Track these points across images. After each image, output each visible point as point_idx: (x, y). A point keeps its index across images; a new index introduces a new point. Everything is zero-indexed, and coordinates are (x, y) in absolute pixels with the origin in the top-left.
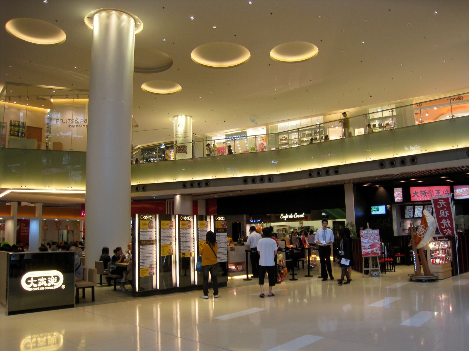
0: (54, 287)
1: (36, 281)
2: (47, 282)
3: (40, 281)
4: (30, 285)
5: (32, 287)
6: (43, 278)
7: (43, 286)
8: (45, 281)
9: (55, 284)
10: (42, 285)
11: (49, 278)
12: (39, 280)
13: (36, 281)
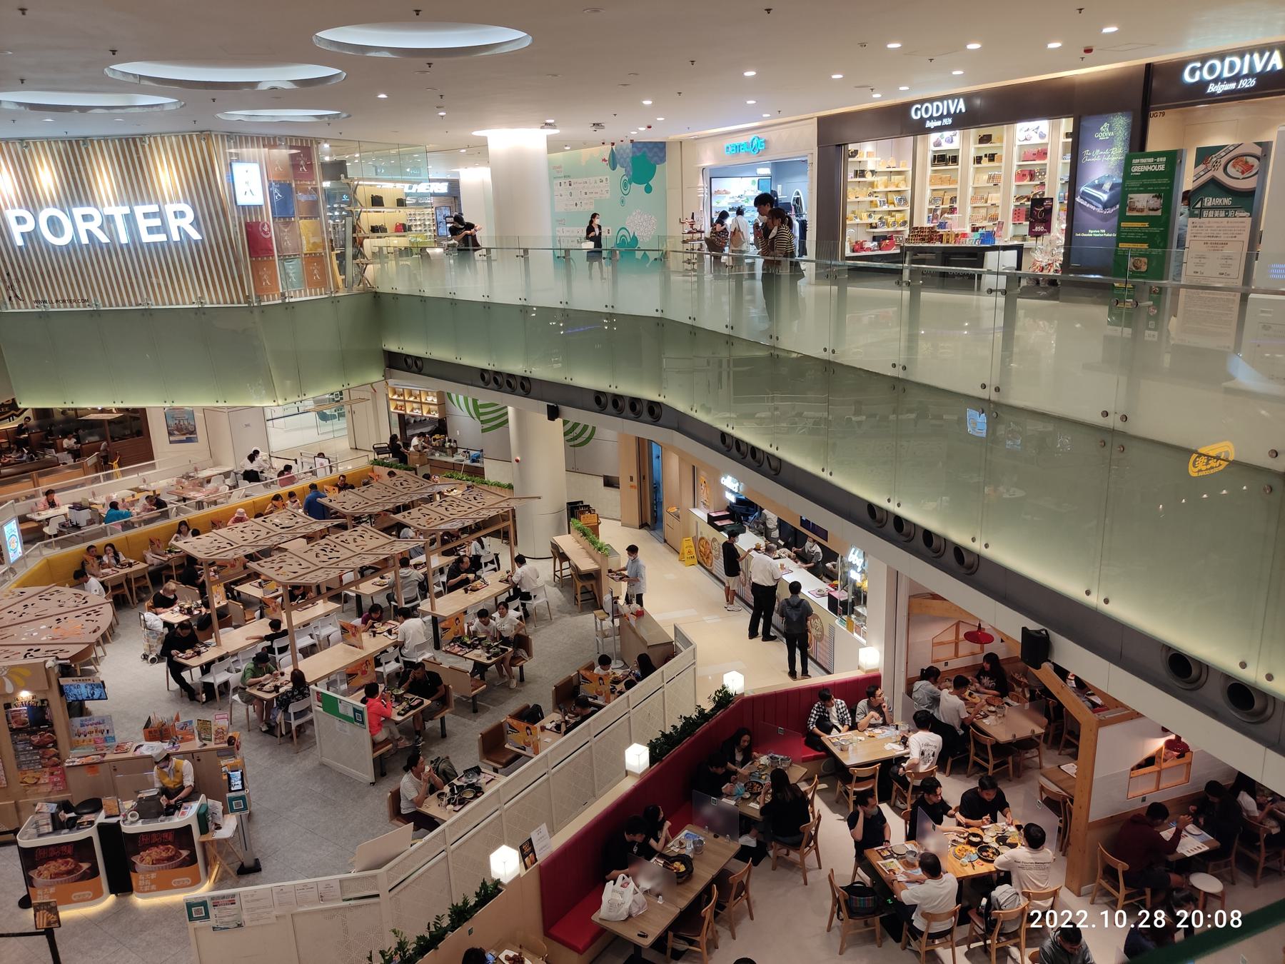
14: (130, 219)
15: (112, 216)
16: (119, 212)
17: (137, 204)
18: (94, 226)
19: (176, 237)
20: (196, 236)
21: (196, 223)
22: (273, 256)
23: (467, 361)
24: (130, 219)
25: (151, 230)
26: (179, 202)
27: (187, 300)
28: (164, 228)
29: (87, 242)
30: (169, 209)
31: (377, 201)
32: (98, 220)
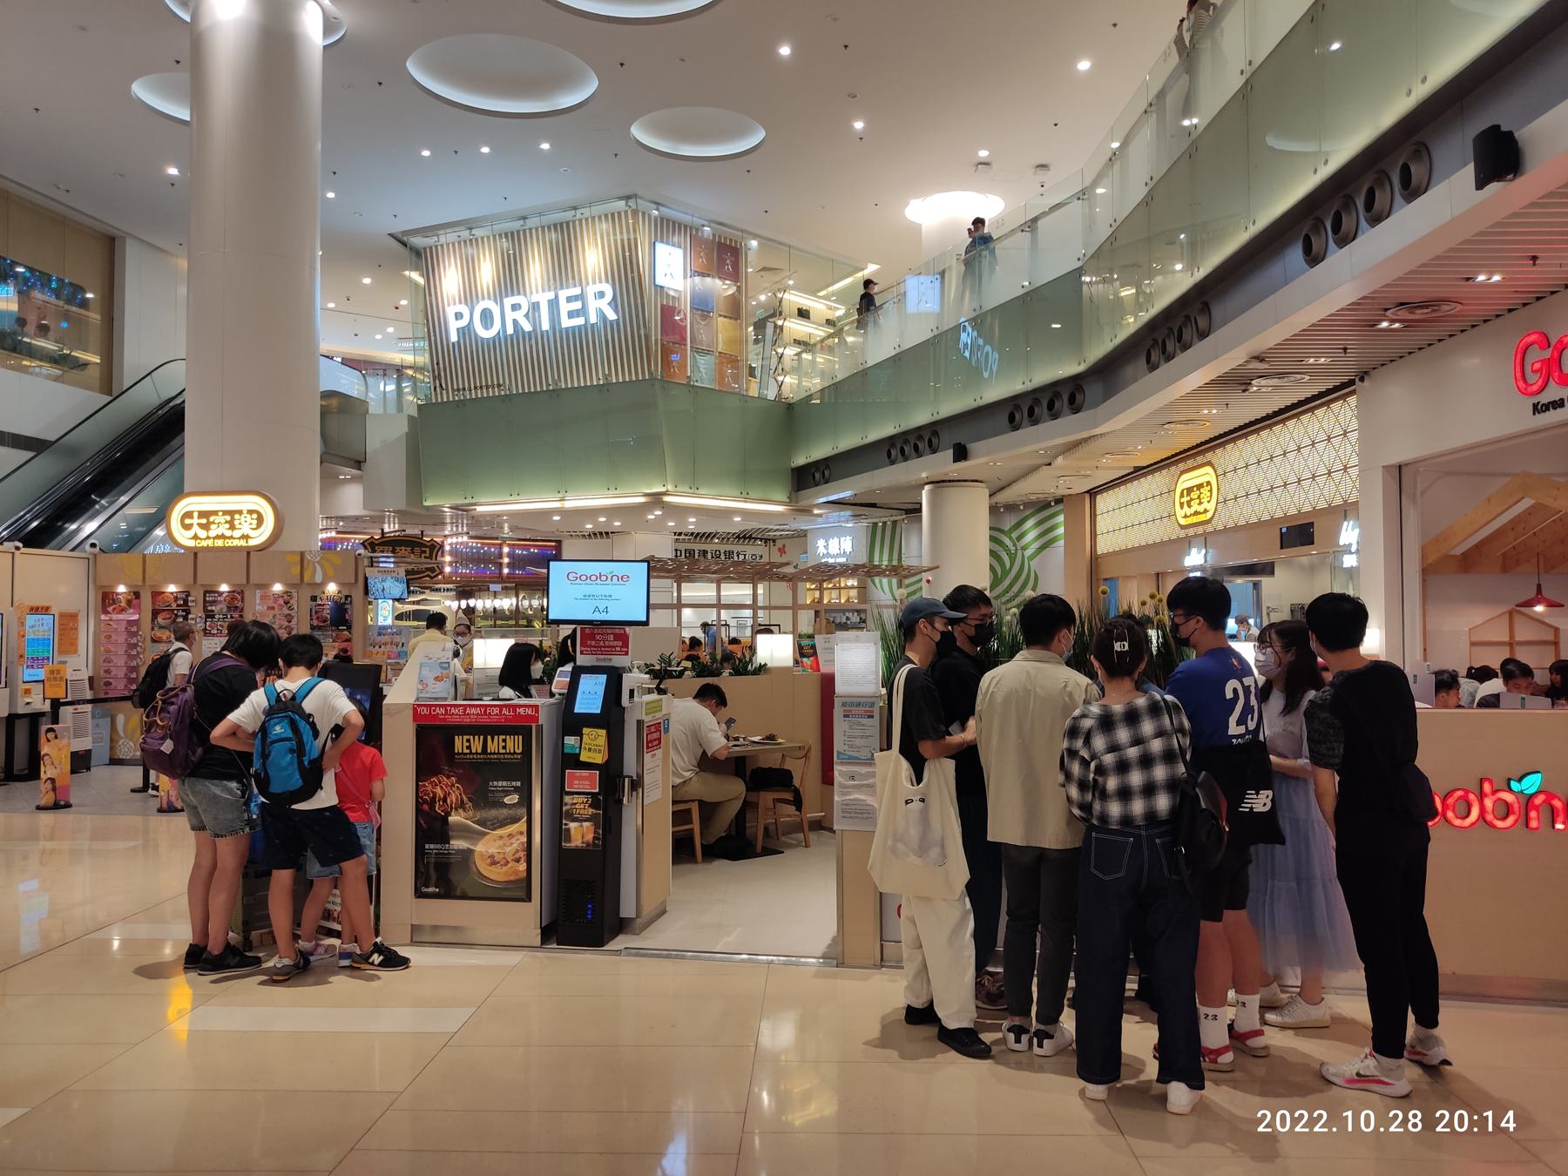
0: (250, 540)
1: (204, 521)
2: (232, 527)
3: (213, 523)
4: (191, 533)
5: (196, 537)
6: (220, 513)
7: (223, 537)
8: (226, 522)
9: (252, 533)
10: (220, 534)
11: (237, 516)
12: (212, 519)
13: (204, 521)
14: (554, 304)
15: (538, 302)
16: (543, 298)
17: (562, 288)
18: (519, 316)
19: (593, 319)
20: (611, 316)
21: (613, 303)
22: (685, 345)
23: (874, 435)
24: (554, 304)
25: (571, 315)
26: (600, 282)
27: (596, 380)
28: (582, 312)
29: (512, 332)
30: (591, 290)
31: (803, 314)
32: (524, 309)
